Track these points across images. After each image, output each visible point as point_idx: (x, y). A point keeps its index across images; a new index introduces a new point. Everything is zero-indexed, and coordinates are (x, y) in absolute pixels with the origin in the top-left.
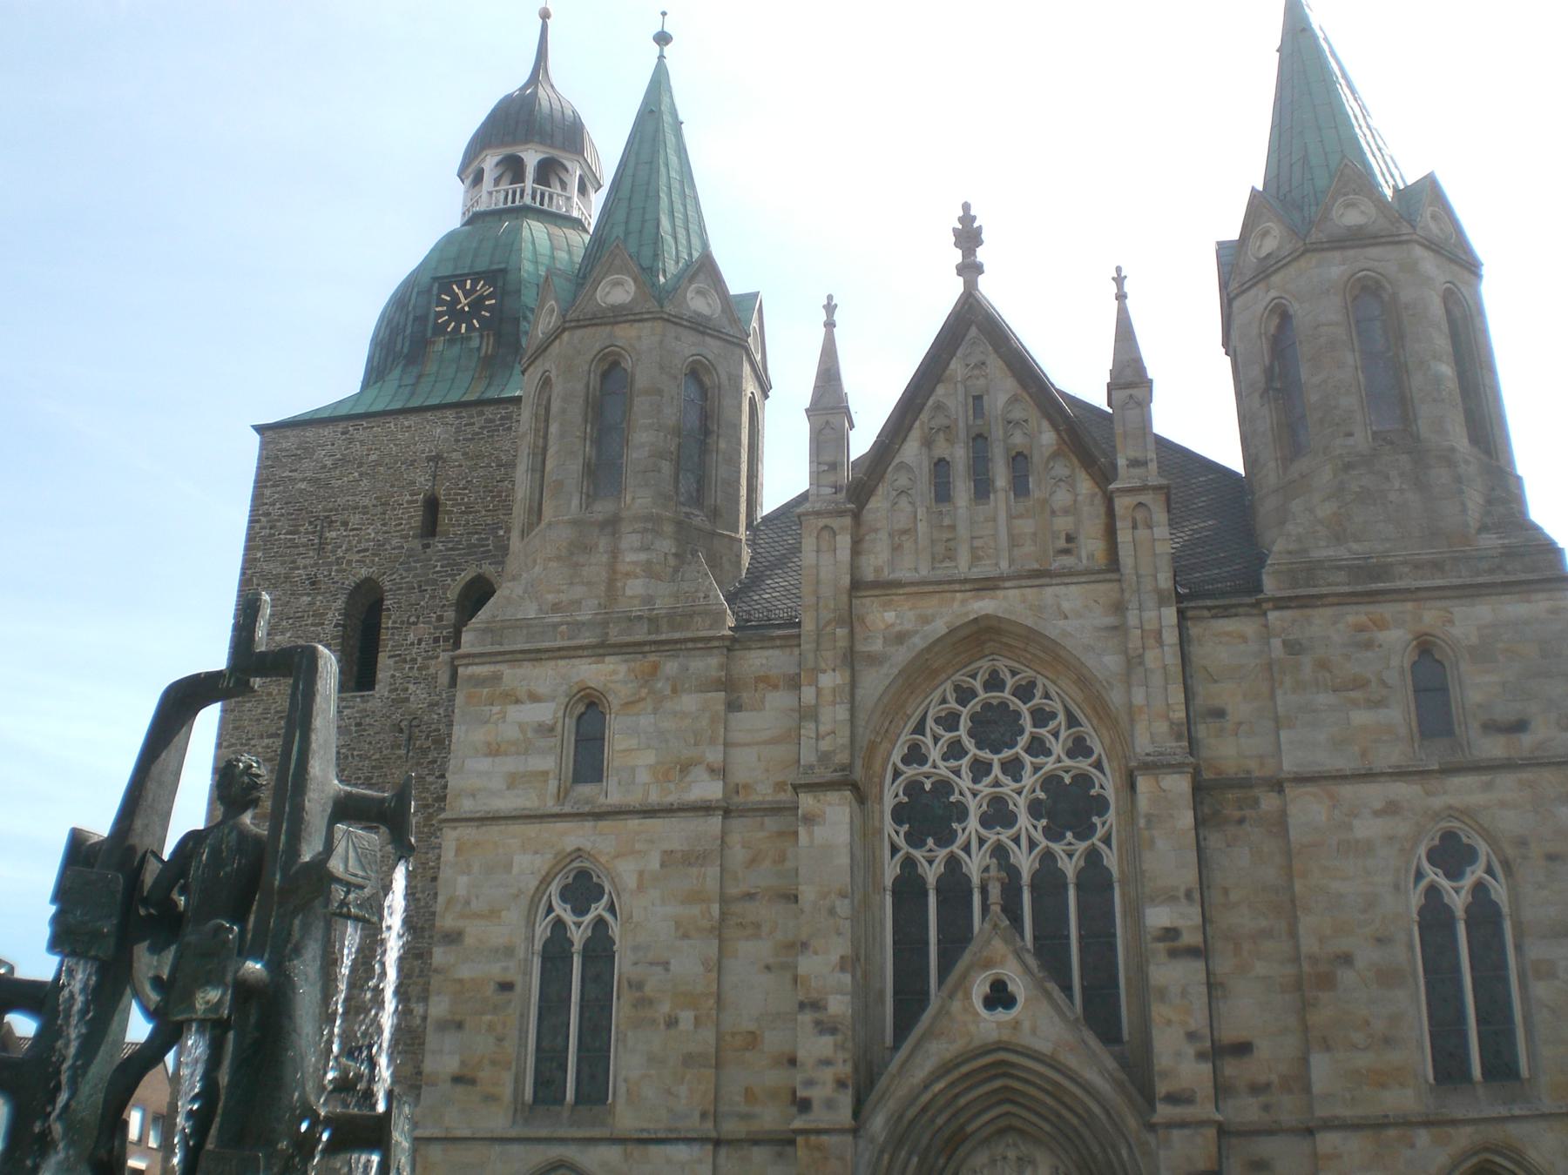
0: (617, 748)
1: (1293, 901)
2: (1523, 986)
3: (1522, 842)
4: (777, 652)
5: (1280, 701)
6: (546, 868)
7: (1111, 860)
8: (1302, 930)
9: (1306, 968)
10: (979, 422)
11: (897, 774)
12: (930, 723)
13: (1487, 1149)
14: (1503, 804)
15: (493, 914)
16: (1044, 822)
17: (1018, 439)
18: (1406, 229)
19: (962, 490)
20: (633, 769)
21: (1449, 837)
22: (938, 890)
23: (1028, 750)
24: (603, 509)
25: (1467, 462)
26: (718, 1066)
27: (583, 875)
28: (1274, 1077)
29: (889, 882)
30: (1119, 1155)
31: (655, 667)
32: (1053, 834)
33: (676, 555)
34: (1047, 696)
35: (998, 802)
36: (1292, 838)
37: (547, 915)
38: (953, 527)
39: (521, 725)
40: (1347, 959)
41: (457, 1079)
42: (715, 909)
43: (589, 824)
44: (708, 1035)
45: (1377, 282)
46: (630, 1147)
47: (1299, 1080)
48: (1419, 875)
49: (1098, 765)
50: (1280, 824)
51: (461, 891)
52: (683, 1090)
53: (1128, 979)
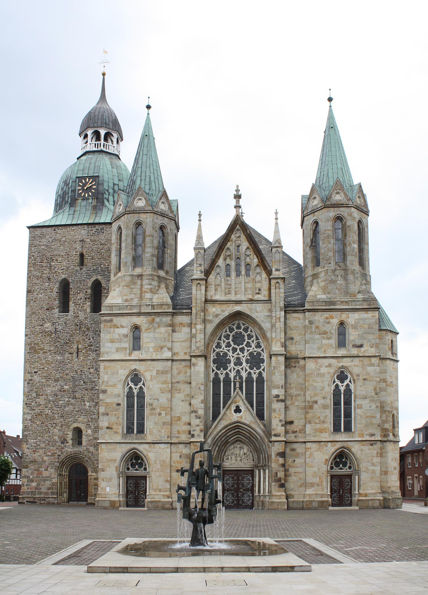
0: (144, 342)
1: (305, 387)
4: (185, 316)
5: (306, 336)
6: (127, 374)
7: (264, 375)
8: (307, 395)
9: (307, 404)
10: (238, 254)
11: (214, 351)
12: (223, 337)
13: (343, 448)
14: (355, 366)
15: (114, 386)
16: (249, 365)
17: (248, 260)
18: (351, 203)
19: (233, 274)
20: (149, 347)
21: (342, 372)
22: (223, 382)
23: (246, 346)
24: (138, 271)
25: (357, 273)
26: (171, 425)
27: (136, 375)
28: (298, 430)
29: (212, 380)
30: (263, 447)
31: (154, 319)
32: (251, 368)
33: (158, 286)
34: (251, 331)
35: (238, 359)
36: (306, 372)
37: (127, 386)
38: (230, 285)
40: (316, 402)
41: (108, 428)
42: (170, 385)
43: (138, 362)
44: (169, 417)
45: (342, 218)
46: (151, 445)
47: (303, 430)
49: (263, 350)
50: (304, 368)
51: (106, 379)
52: (163, 431)
53: (267, 405)
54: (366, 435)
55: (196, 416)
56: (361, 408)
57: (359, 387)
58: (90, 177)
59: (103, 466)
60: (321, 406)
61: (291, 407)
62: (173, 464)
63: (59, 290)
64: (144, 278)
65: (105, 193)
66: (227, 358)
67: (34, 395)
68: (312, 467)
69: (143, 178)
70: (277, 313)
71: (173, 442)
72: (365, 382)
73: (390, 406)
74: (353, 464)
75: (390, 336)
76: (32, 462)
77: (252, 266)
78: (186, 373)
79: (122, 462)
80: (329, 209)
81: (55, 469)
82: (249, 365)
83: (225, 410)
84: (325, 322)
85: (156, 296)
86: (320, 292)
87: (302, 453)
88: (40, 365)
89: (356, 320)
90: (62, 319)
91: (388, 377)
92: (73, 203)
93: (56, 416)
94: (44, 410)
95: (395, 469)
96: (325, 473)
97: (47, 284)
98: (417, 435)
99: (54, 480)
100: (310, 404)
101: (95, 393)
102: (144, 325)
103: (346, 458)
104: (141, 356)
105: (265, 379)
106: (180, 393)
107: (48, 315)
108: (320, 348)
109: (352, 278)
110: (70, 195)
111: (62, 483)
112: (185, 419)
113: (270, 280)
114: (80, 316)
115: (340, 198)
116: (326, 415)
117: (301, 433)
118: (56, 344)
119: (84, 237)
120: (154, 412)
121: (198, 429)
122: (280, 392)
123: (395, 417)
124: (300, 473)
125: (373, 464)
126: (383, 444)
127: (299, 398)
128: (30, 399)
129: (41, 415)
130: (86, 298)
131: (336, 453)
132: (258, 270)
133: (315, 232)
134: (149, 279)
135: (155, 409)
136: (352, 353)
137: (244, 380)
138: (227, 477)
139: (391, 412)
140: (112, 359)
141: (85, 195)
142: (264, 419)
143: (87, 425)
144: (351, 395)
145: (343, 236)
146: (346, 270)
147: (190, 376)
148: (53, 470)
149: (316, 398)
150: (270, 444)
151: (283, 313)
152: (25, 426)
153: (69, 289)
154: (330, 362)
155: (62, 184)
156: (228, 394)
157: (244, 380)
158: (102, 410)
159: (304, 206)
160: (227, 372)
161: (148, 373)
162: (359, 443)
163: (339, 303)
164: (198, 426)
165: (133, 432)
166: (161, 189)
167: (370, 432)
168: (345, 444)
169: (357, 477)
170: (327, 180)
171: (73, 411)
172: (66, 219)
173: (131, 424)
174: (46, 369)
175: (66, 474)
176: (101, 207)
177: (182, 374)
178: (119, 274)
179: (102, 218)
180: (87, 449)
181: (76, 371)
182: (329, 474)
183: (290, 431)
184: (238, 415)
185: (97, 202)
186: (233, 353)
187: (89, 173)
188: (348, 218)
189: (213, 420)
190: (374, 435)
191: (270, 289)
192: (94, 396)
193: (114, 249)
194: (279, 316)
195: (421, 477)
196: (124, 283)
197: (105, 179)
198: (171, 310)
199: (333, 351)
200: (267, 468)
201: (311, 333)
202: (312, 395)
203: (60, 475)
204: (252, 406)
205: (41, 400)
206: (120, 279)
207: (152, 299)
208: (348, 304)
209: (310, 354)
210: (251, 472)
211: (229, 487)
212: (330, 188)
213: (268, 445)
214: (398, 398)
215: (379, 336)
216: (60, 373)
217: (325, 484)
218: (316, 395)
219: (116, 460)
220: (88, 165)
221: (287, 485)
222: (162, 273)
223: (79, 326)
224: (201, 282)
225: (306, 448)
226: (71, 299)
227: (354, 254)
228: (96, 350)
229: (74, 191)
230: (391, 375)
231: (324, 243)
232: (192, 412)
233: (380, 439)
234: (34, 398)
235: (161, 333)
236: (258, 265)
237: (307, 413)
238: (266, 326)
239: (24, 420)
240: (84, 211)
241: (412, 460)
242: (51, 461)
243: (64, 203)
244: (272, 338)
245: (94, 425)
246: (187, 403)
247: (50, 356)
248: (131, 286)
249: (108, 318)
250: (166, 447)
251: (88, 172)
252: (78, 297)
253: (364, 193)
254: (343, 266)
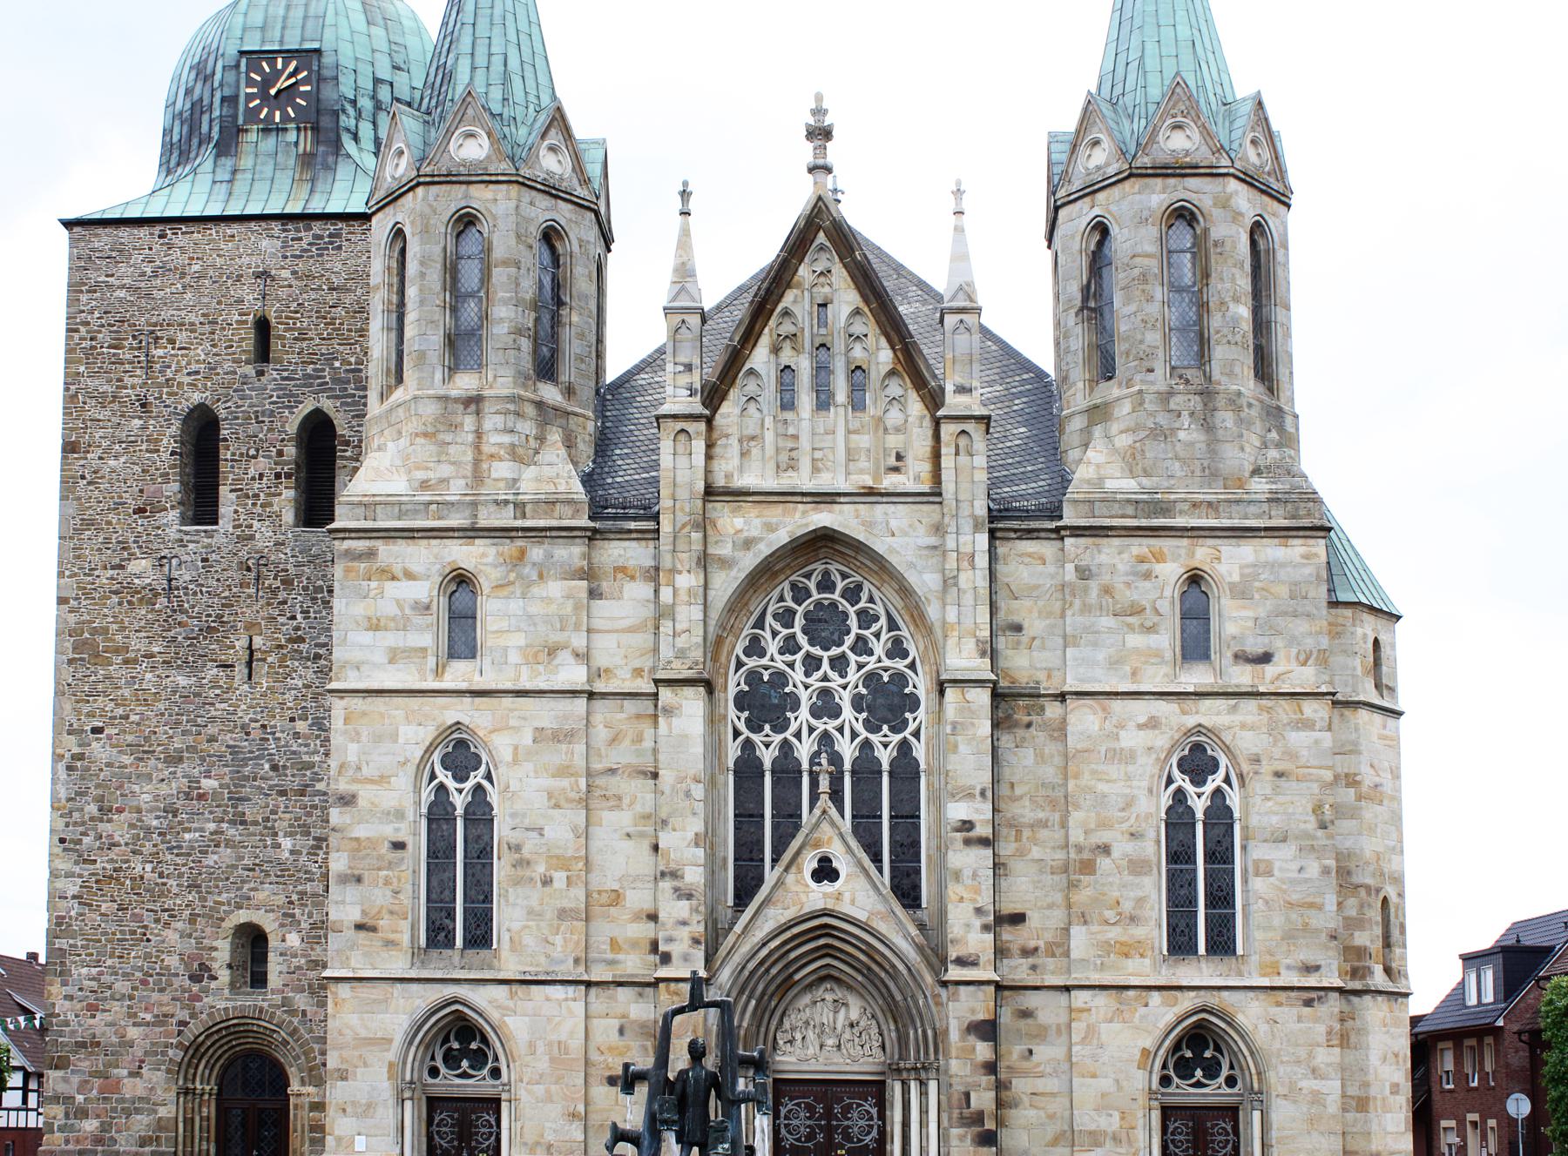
1: (1066, 797)
2: (1245, 881)
3: (1256, 760)
4: (634, 544)
5: (1068, 620)
7: (920, 751)
9: (1073, 855)
10: (823, 331)
11: (740, 664)
12: (769, 619)
14: (1243, 726)
15: (382, 780)
16: (865, 715)
17: (858, 352)
18: (1225, 162)
19: (806, 400)
20: (506, 649)
21: (1198, 748)
22: (773, 772)
23: (852, 649)
24: (466, 383)
25: (1250, 405)
27: (461, 744)
28: (1041, 943)
29: (731, 765)
32: (872, 727)
34: (871, 600)
35: (825, 693)
38: (796, 437)
39: (398, 602)
40: (1105, 849)
41: (359, 927)
42: (583, 782)
43: (467, 700)
44: (580, 893)
45: (1192, 214)
46: (515, 987)
47: (1060, 947)
48: (1170, 781)
49: (912, 666)
50: (1060, 730)
51: (352, 758)
53: (929, 857)
54: (1289, 967)
55: (676, 890)
56: (1270, 873)
57: (1258, 800)
58: (289, 54)
59: (343, 1060)
60: (1125, 863)
61: (1017, 866)
62: (595, 1056)
63: (182, 443)
64: (488, 407)
65: (344, 111)
66: (787, 690)
67: (92, 809)
68: (1094, 1076)
69: (481, 60)
70: (962, 539)
71: (593, 979)
72: (1282, 782)
73: (1371, 868)
74: (1242, 1069)
75: (1368, 627)
76: (83, 1045)
77: (873, 375)
78: (639, 739)
79: (413, 1049)
80: (1147, 180)
81: (168, 1071)
82: (865, 715)
83: (779, 869)
84: (1135, 574)
85: (530, 473)
86: (1115, 469)
87: (1058, 1026)
88: (112, 704)
89: (1247, 566)
90: (191, 546)
91: (1365, 769)
92: (228, 143)
93: (172, 882)
94: (127, 861)
95: (1395, 1089)
96: (1142, 1100)
97: (137, 422)
98: (1473, 977)
99: (163, 1112)
100: (1086, 855)
101: (314, 807)
102: (488, 569)
103: (1218, 1049)
104: (477, 678)
105: (923, 766)
106: (619, 807)
107: (140, 529)
108: (1117, 662)
109: (1229, 424)
110: (216, 113)
111: (193, 1119)
112: (638, 899)
113: (937, 423)
114: (258, 536)
115: (1187, 145)
116: (1140, 894)
117: (1053, 955)
118: (172, 634)
119: (272, 264)
120: (528, 873)
121: (684, 934)
122: (979, 813)
123: (1392, 910)
124: (1053, 1095)
125: (1314, 1071)
126: (1349, 1001)
127: (1043, 834)
128: (75, 824)
129: (117, 879)
130: (278, 476)
131: (1180, 1028)
132: (895, 388)
133: (1098, 262)
134: (506, 413)
135: (528, 863)
136: (1234, 681)
137: (847, 766)
138: (790, 1106)
139: (1378, 891)
140: (376, 686)
141: (270, 115)
142: (919, 906)
143: (285, 915)
144: (1231, 826)
145: (1199, 277)
146: (1207, 394)
147: (655, 751)
148: (159, 1076)
149: (1103, 837)
150: (943, 993)
151: (983, 539)
152: (58, 917)
153: (218, 440)
154: (1155, 713)
155: (187, 77)
156: (791, 816)
157: (847, 766)
158: (338, 863)
159: (1057, 169)
160: (785, 741)
161: (503, 736)
162: (1262, 995)
163: (1185, 507)
164: (684, 923)
165: (450, 943)
166: (546, 100)
167: (1302, 957)
168: (1212, 1000)
169: (1257, 1115)
170: (1141, 82)
171: (236, 867)
172: (205, 197)
173: (444, 914)
174: (133, 718)
175: (208, 1088)
176: (331, 159)
177: (627, 742)
178: (399, 394)
179: (334, 196)
180: (286, 1002)
181: (243, 727)
182: (1155, 1104)
183: (1015, 948)
184: (826, 887)
185: (317, 142)
186: (807, 674)
187: (286, 39)
188: (1217, 213)
189: (736, 905)
190: (1317, 968)
191: (936, 456)
192: (309, 814)
193: (380, 307)
194: (969, 549)
195: (1492, 1123)
196: (413, 426)
197: (342, 61)
198: (584, 522)
199: (1166, 675)
200: (933, 1074)
201: (1086, 609)
202: (1093, 826)
203: (187, 1092)
204: (877, 859)
205: (118, 828)
206: (400, 410)
207: (515, 481)
208: (1217, 510)
209: (1082, 681)
210: (875, 1090)
211: (798, 1140)
212: (1152, 108)
213: (936, 996)
214: (1401, 842)
215: (1330, 624)
216: (184, 733)
217: (1141, 1137)
218: (1104, 825)
219: (390, 1041)
220: (281, 12)
221: (1005, 1136)
222: (550, 393)
223: (255, 569)
224: (692, 427)
225: (1071, 1010)
226: (226, 478)
227: (1238, 338)
228: (317, 657)
229: (230, 101)
230: (1376, 762)
231: (1128, 300)
232: (663, 874)
233: (1338, 983)
234: (92, 819)
235: (548, 600)
236: (892, 373)
237: (1072, 885)
238: (924, 581)
239: (55, 897)
240: (268, 170)
241: (1458, 1061)
242: (153, 1044)
243: (195, 141)
244: (944, 622)
245: (310, 915)
246: (646, 845)
247: (149, 676)
248: (441, 436)
249: (360, 545)
251: (282, 36)
252: (252, 472)
253: (1274, 127)
254: (1197, 381)
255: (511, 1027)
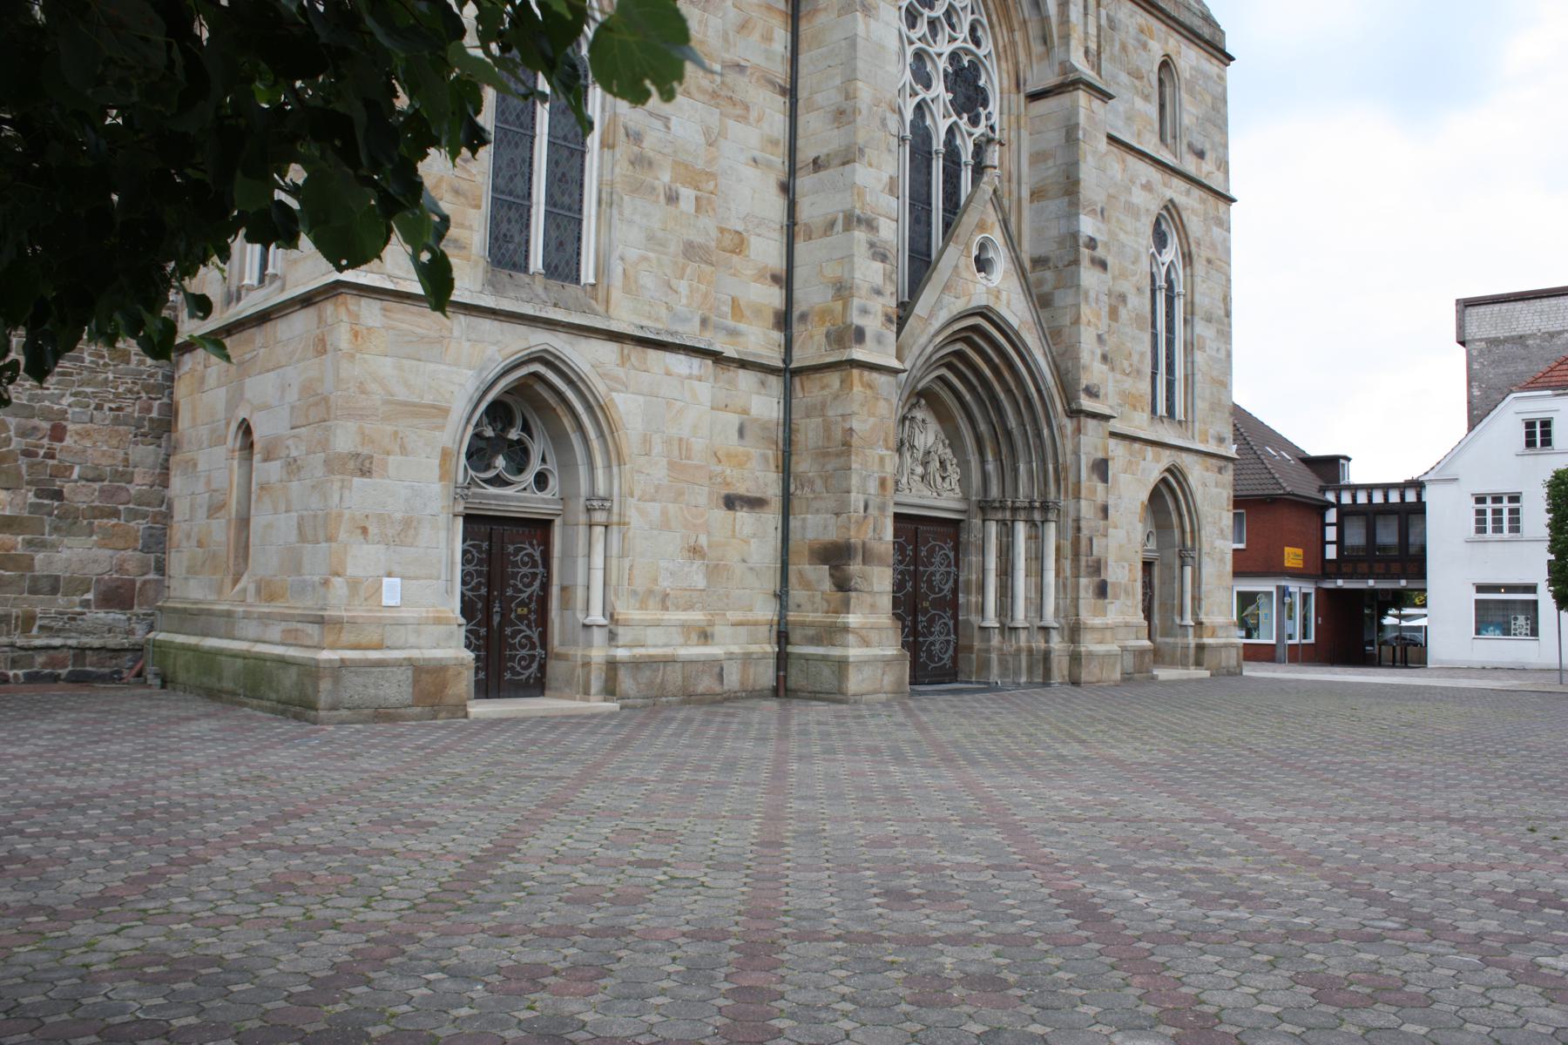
52: (683, 286)
55: (872, 245)
219: (444, 412)
250: (695, 372)
255: (621, 407)
